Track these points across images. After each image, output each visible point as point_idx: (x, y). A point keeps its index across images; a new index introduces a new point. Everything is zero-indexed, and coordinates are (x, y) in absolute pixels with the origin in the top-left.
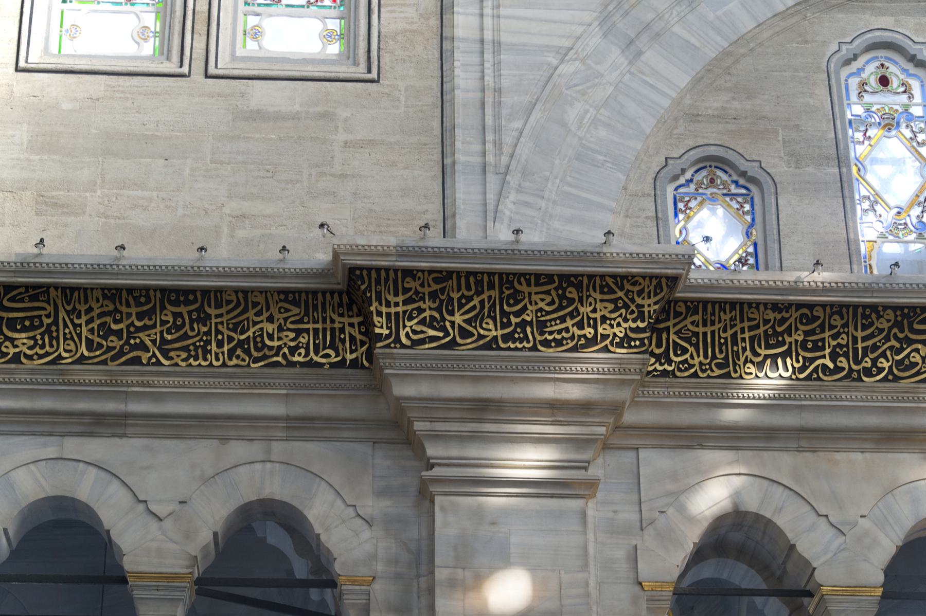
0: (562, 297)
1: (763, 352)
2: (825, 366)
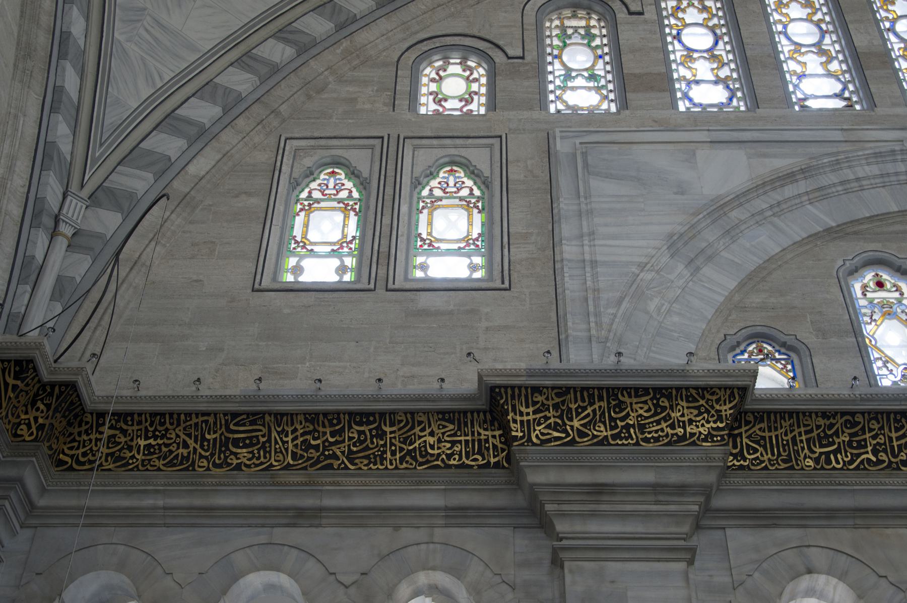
0: (656, 406)
1: (818, 450)
2: (869, 460)
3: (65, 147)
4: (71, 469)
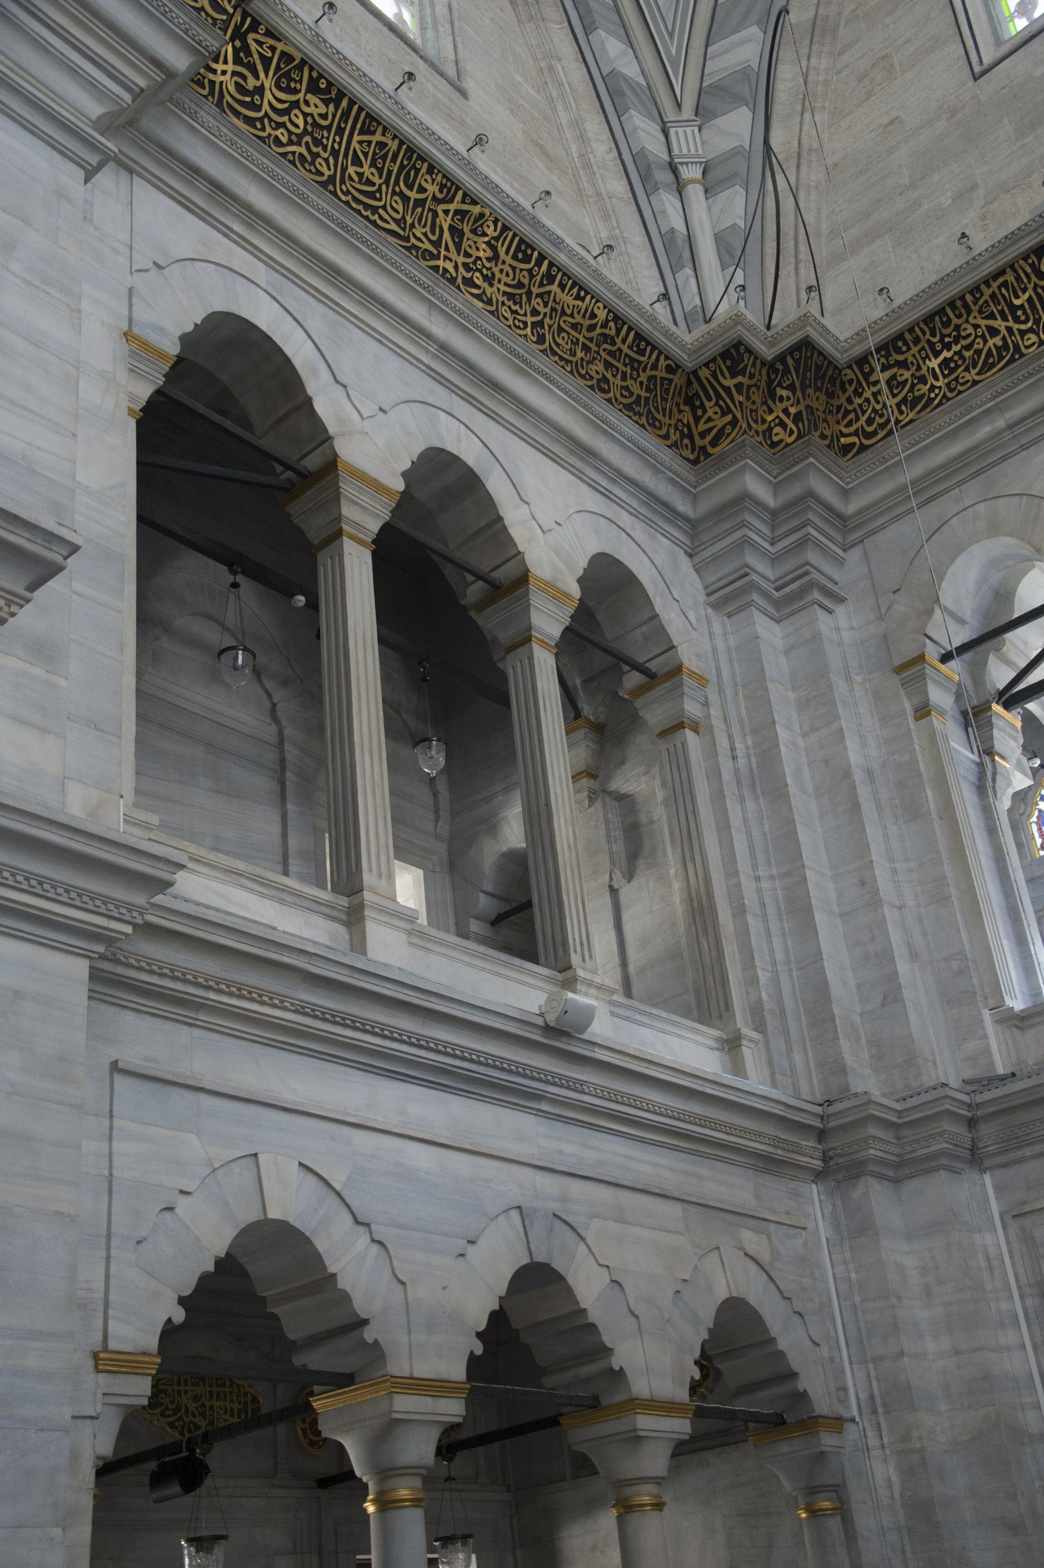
3: (631, 70)
4: (863, 448)
